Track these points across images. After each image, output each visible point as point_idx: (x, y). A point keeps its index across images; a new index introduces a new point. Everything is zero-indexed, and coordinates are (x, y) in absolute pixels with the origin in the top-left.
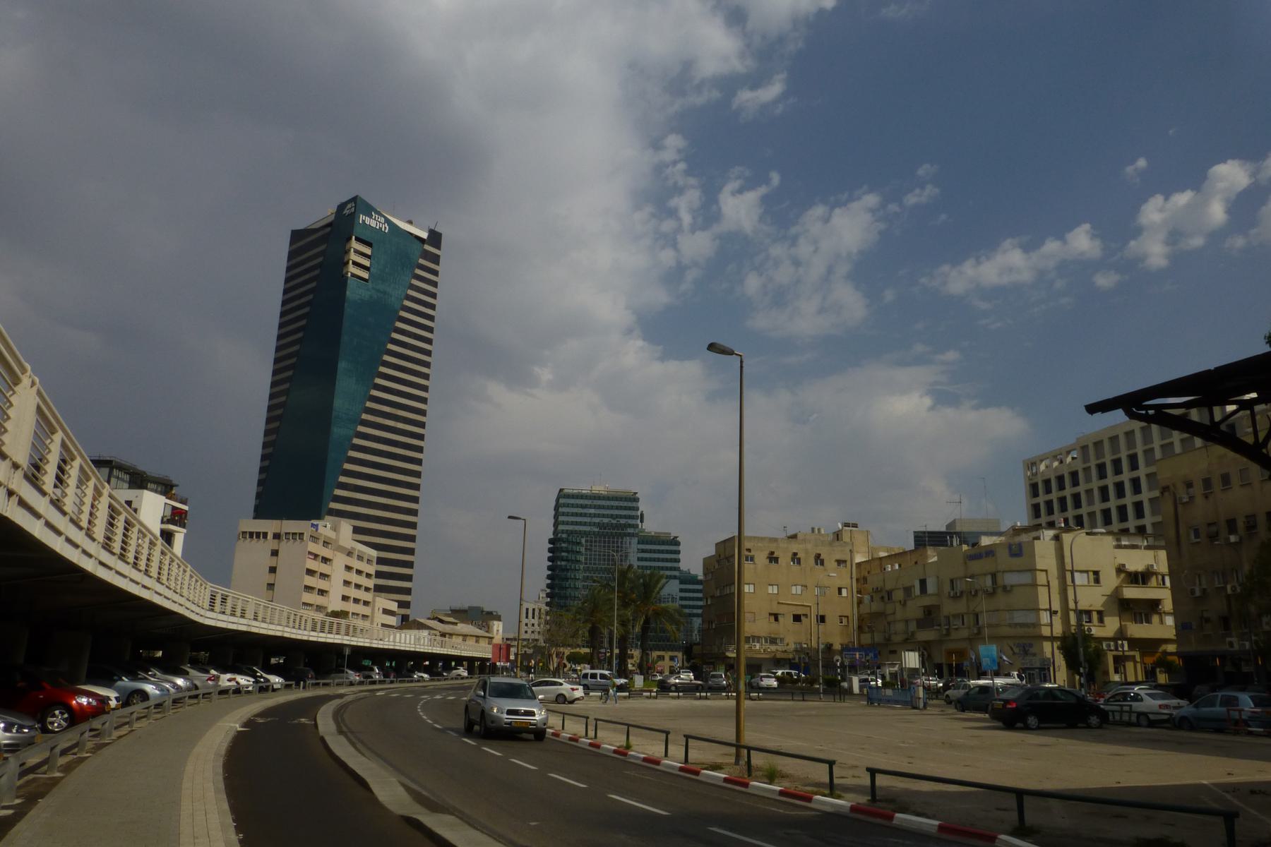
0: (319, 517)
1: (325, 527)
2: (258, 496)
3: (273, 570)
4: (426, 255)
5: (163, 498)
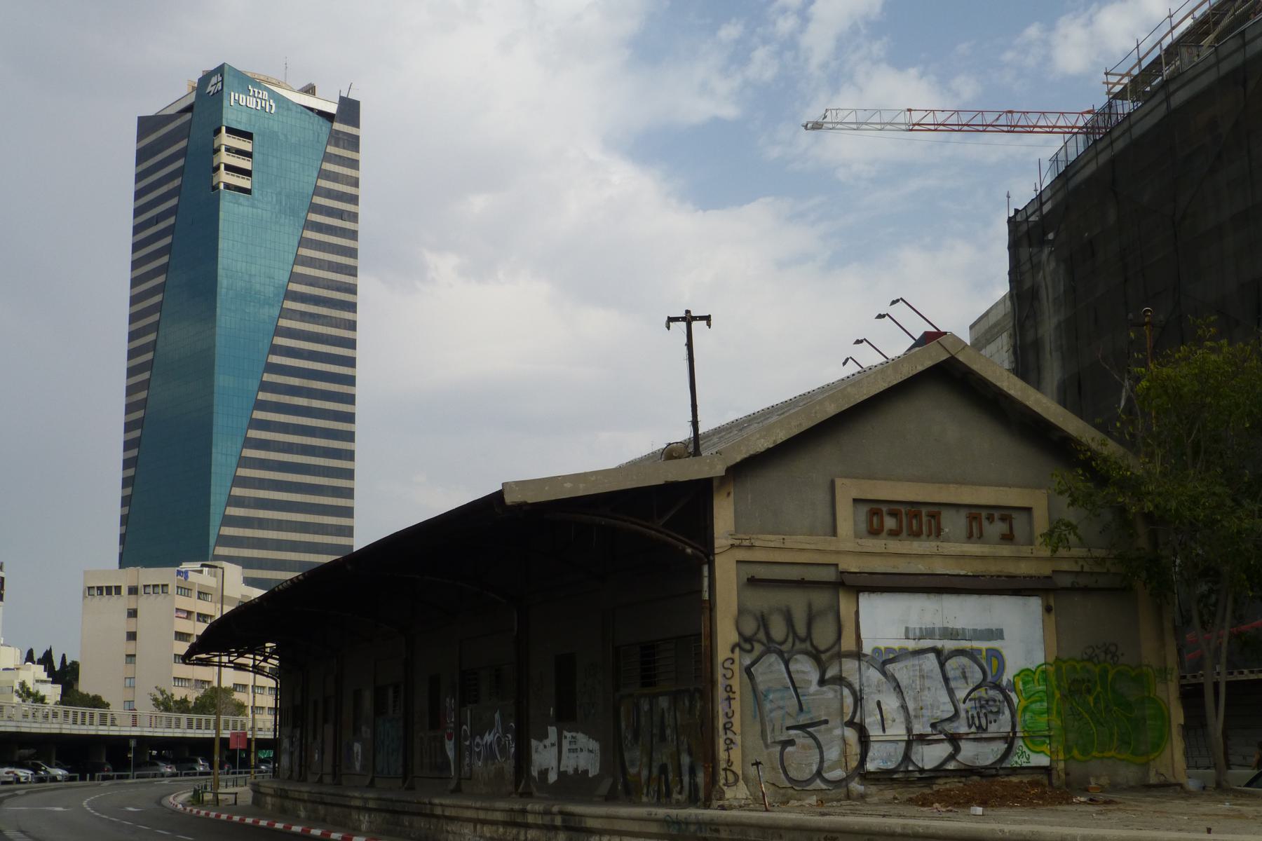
0: (201, 553)
2: (125, 520)
3: (132, 636)
4: (336, 138)
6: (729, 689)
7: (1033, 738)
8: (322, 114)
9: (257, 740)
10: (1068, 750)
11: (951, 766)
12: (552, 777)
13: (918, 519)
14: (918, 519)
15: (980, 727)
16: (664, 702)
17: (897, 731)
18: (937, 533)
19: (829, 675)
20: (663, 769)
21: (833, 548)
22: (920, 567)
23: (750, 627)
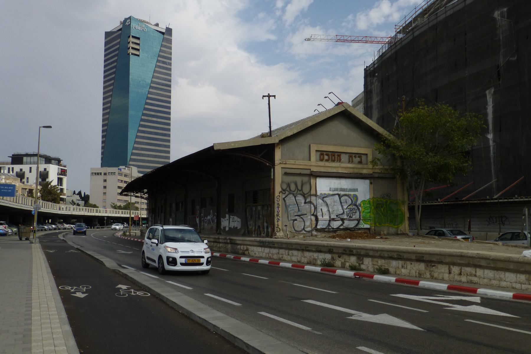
0: (126, 164)
1: (125, 170)
2: (102, 153)
3: (105, 187)
5: (57, 167)
6: (278, 204)
7: (365, 220)
8: (160, 32)
9: (142, 218)
10: (375, 223)
11: (342, 227)
12: (227, 229)
13: (335, 156)
14: (335, 156)
15: (350, 217)
16: (259, 208)
17: (327, 217)
18: (340, 160)
19: (307, 201)
20: (259, 227)
21: (309, 164)
22: (334, 170)
23: (285, 187)
